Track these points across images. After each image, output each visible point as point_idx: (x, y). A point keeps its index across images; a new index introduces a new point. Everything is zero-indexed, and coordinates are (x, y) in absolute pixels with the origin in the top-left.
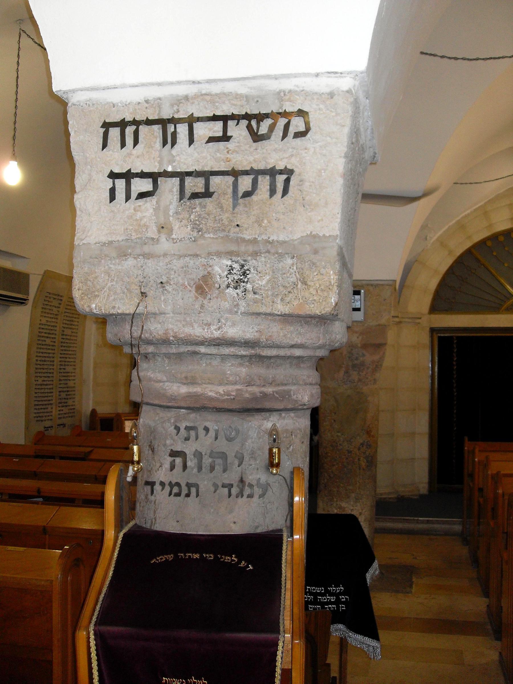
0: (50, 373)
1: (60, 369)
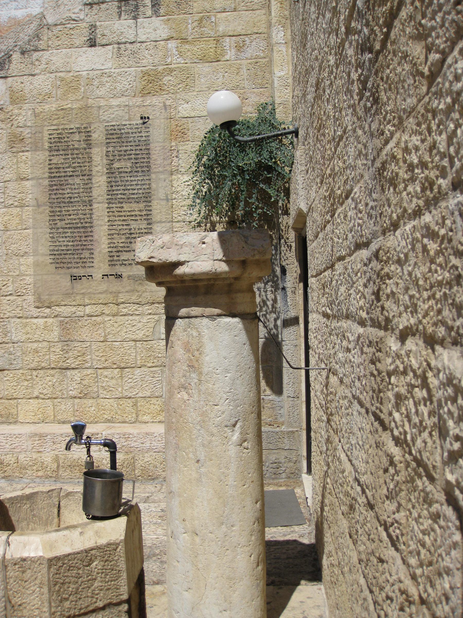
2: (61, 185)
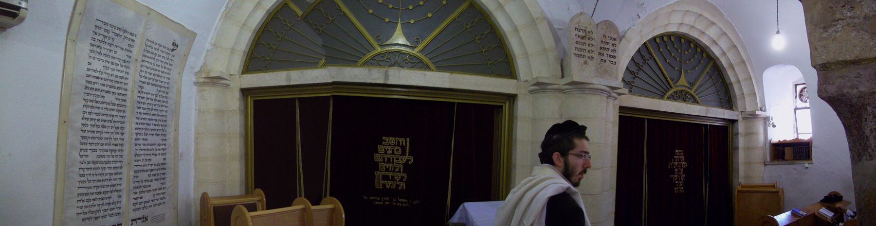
0: (116, 145)
1: (137, 139)
2: (97, 102)
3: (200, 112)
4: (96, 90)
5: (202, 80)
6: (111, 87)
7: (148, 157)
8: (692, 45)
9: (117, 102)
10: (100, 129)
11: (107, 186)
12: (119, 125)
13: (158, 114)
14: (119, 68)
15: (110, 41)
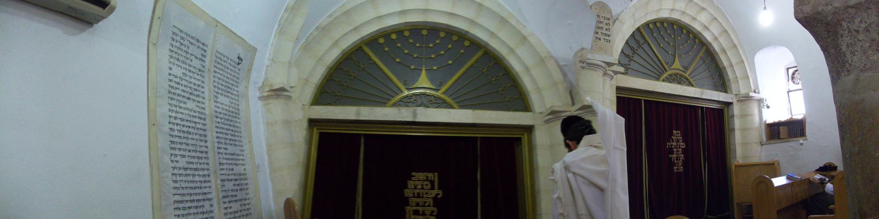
0: (202, 152)
1: (219, 148)
2: (180, 107)
3: (268, 124)
4: (178, 95)
5: (266, 94)
6: (191, 94)
7: (231, 167)
8: (685, 31)
9: (197, 109)
10: (186, 135)
11: (199, 194)
12: (201, 132)
13: (231, 128)
14: (195, 76)
15: (186, 49)
